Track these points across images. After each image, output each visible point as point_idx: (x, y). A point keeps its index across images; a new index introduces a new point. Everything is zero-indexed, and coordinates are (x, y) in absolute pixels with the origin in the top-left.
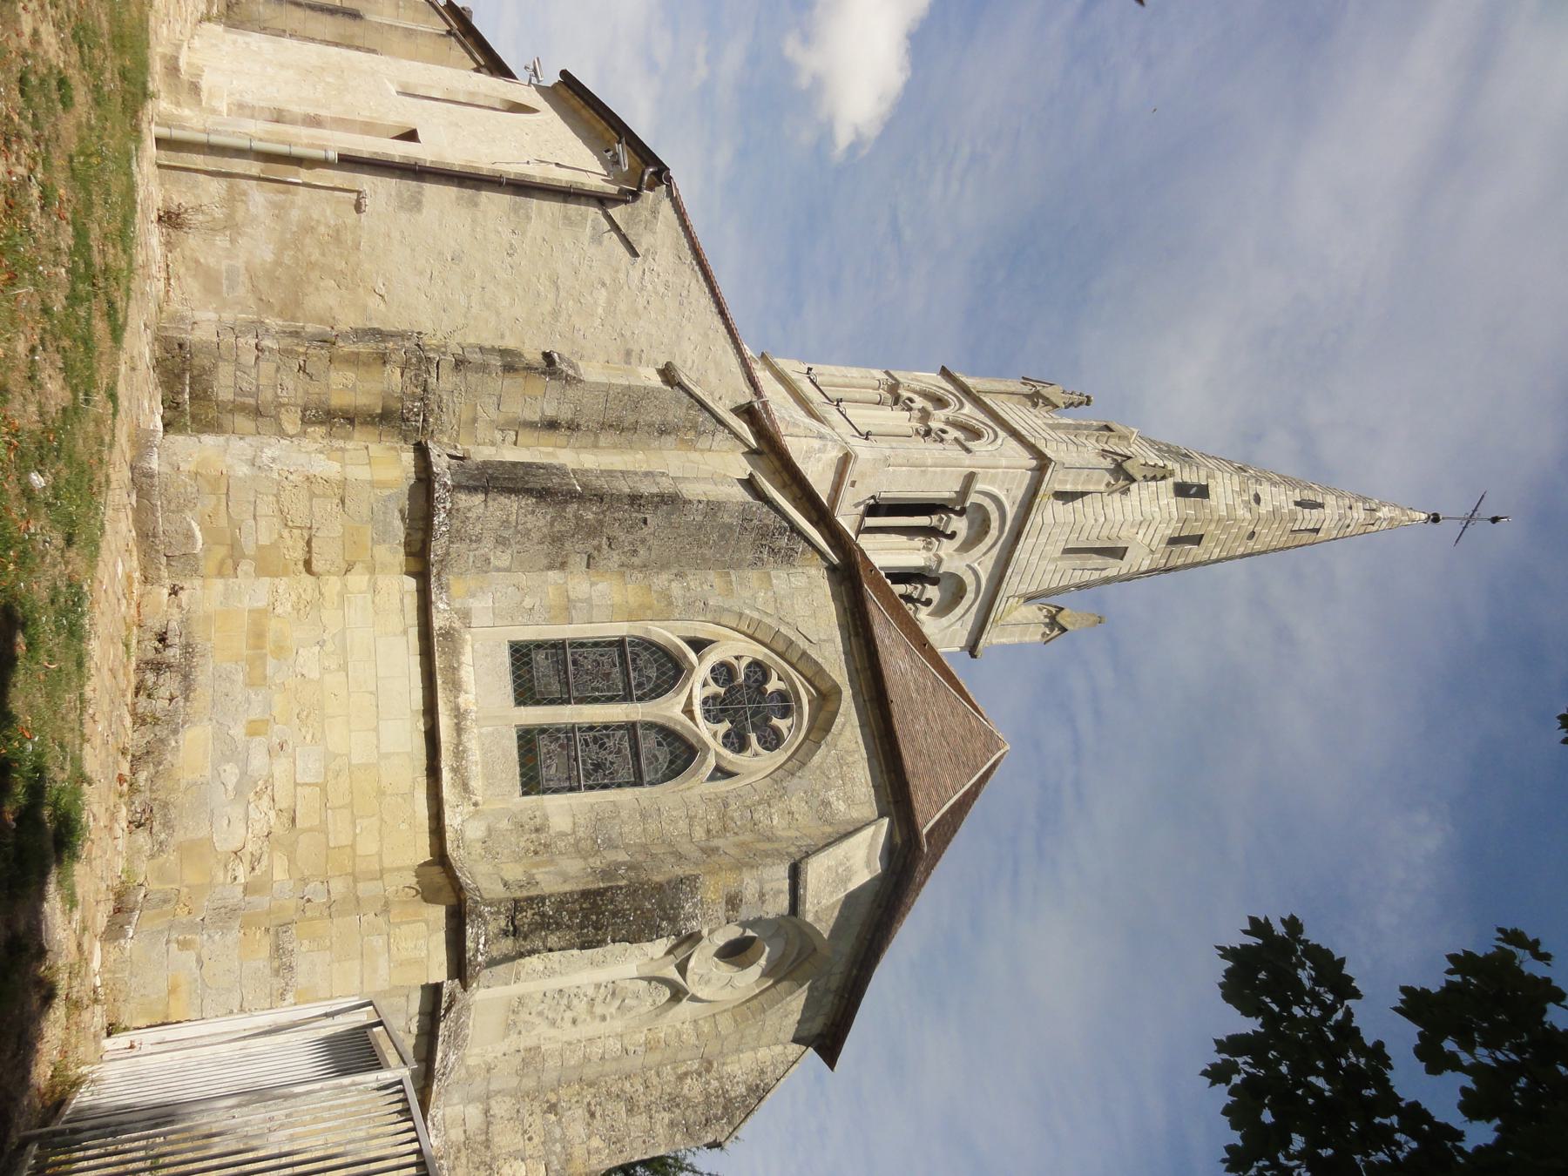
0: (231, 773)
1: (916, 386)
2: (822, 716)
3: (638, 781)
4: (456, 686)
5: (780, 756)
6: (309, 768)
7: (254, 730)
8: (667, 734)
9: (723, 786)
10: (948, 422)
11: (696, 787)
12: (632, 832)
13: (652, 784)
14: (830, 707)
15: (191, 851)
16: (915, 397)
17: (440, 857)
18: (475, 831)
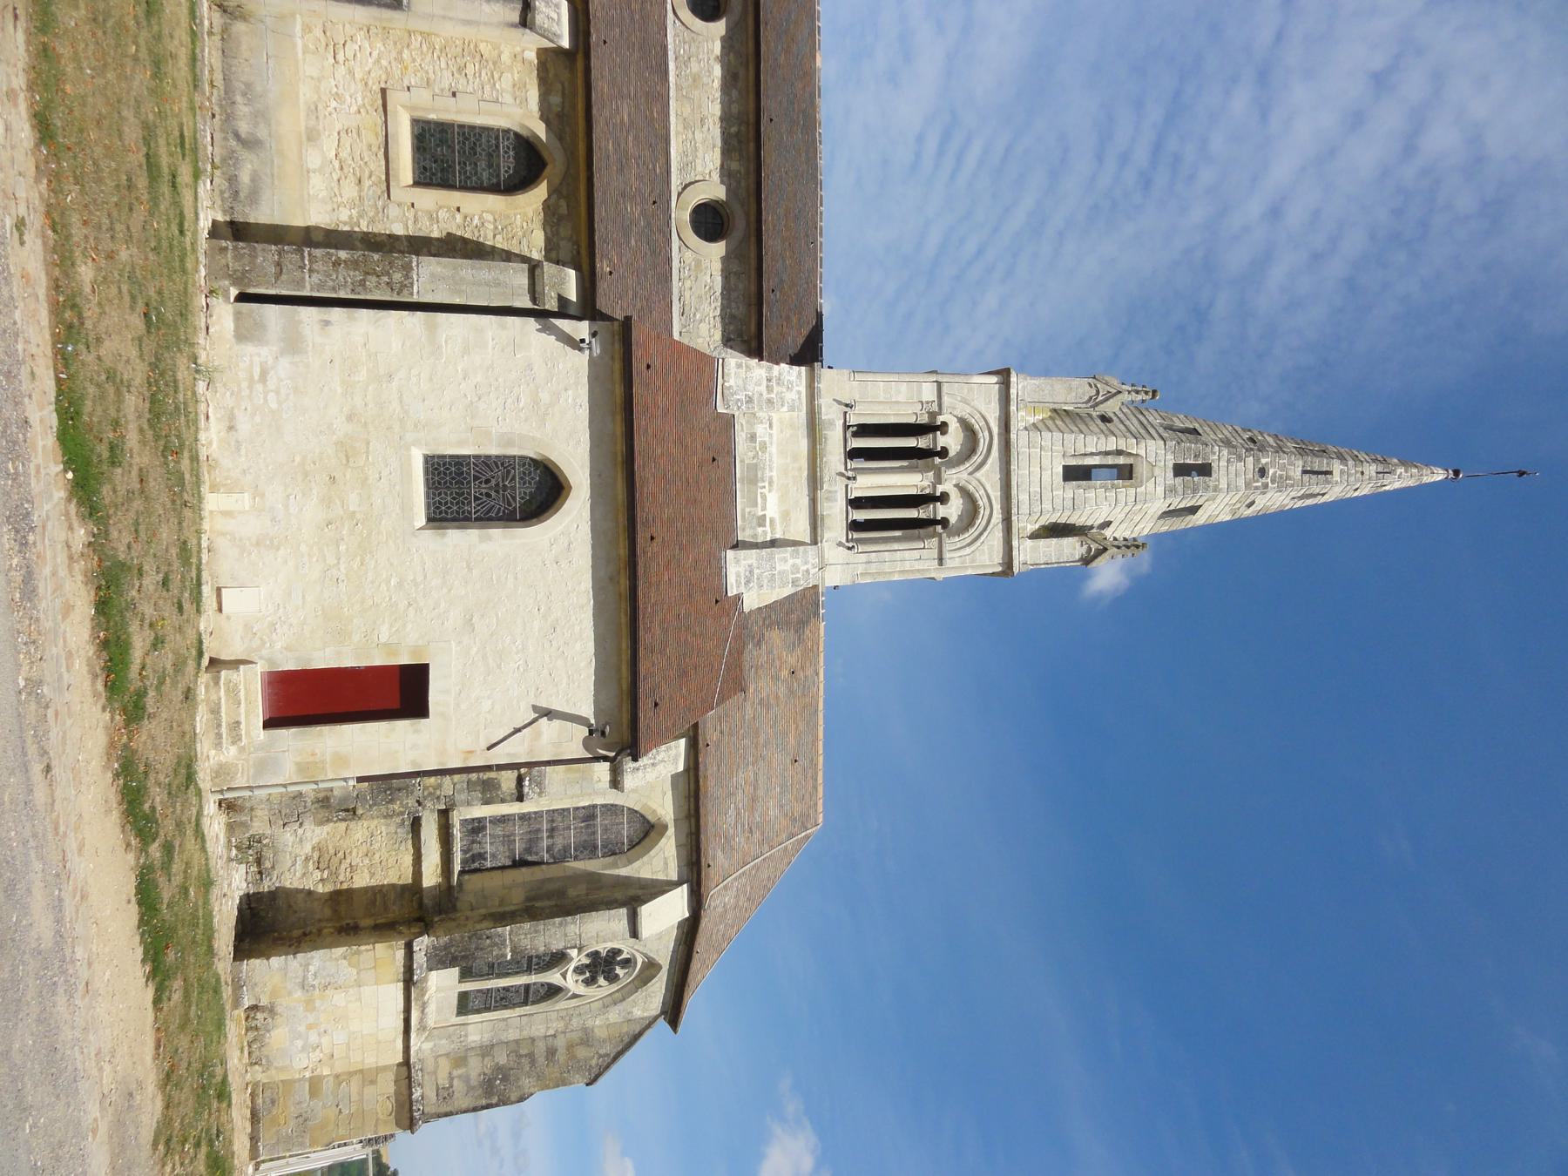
0: (299, 1043)
1: (963, 411)
2: (647, 973)
3: (525, 1003)
4: (423, 992)
5: (614, 987)
6: (340, 1037)
7: (310, 1027)
8: (550, 986)
9: (574, 1003)
10: (957, 486)
11: (561, 1004)
12: (512, 1035)
13: (534, 1003)
14: (653, 971)
15: (281, 1069)
16: (954, 426)
17: (406, 1063)
18: (428, 1046)
